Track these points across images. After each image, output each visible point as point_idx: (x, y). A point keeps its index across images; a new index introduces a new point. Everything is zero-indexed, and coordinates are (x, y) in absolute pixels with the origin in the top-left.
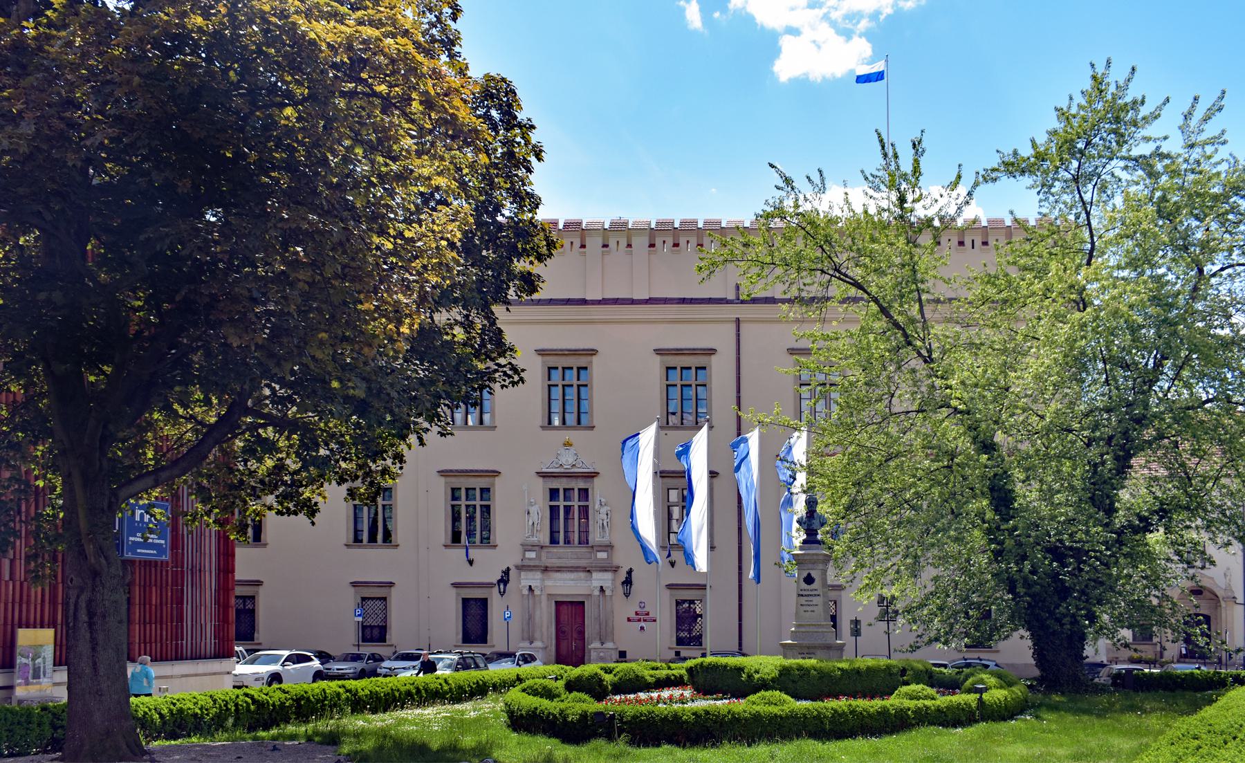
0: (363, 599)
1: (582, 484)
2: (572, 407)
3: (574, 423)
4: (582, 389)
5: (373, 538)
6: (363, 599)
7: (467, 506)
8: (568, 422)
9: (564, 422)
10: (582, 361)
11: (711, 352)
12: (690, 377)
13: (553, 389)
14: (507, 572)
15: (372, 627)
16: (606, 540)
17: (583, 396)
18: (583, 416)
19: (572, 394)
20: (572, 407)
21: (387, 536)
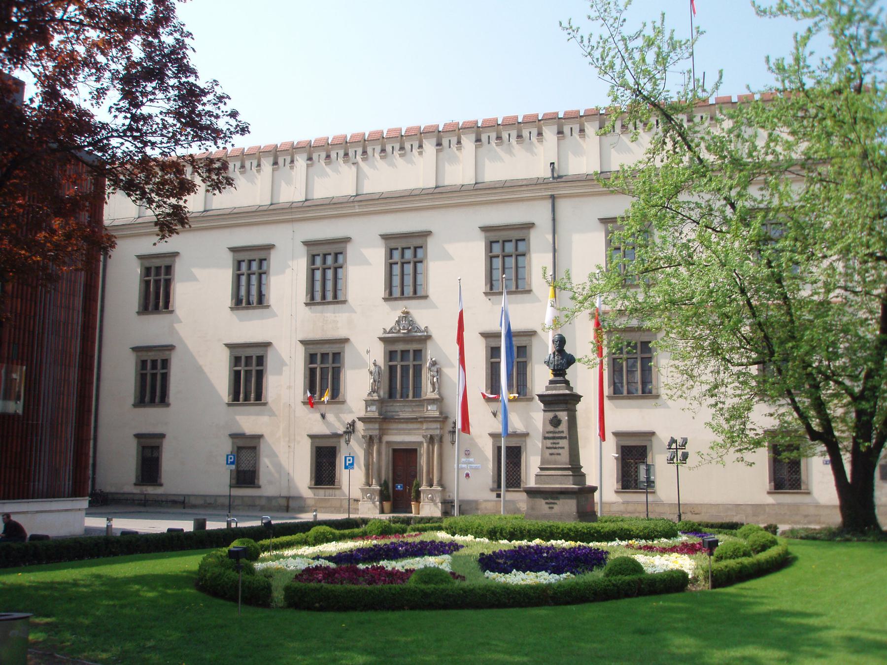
0: (240, 449)
1: (416, 346)
2: (409, 280)
3: (411, 294)
4: (419, 265)
5: (247, 398)
6: (240, 449)
7: (333, 368)
8: (406, 295)
9: (402, 293)
10: (417, 242)
11: (530, 226)
12: (510, 248)
13: (394, 266)
14: (353, 424)
15: (244, 472)
16: (435, 396)
17: (419, 270)
18: (418, 288)
19: (409, 269)
20: (409, 280)
21: (259, 397)
